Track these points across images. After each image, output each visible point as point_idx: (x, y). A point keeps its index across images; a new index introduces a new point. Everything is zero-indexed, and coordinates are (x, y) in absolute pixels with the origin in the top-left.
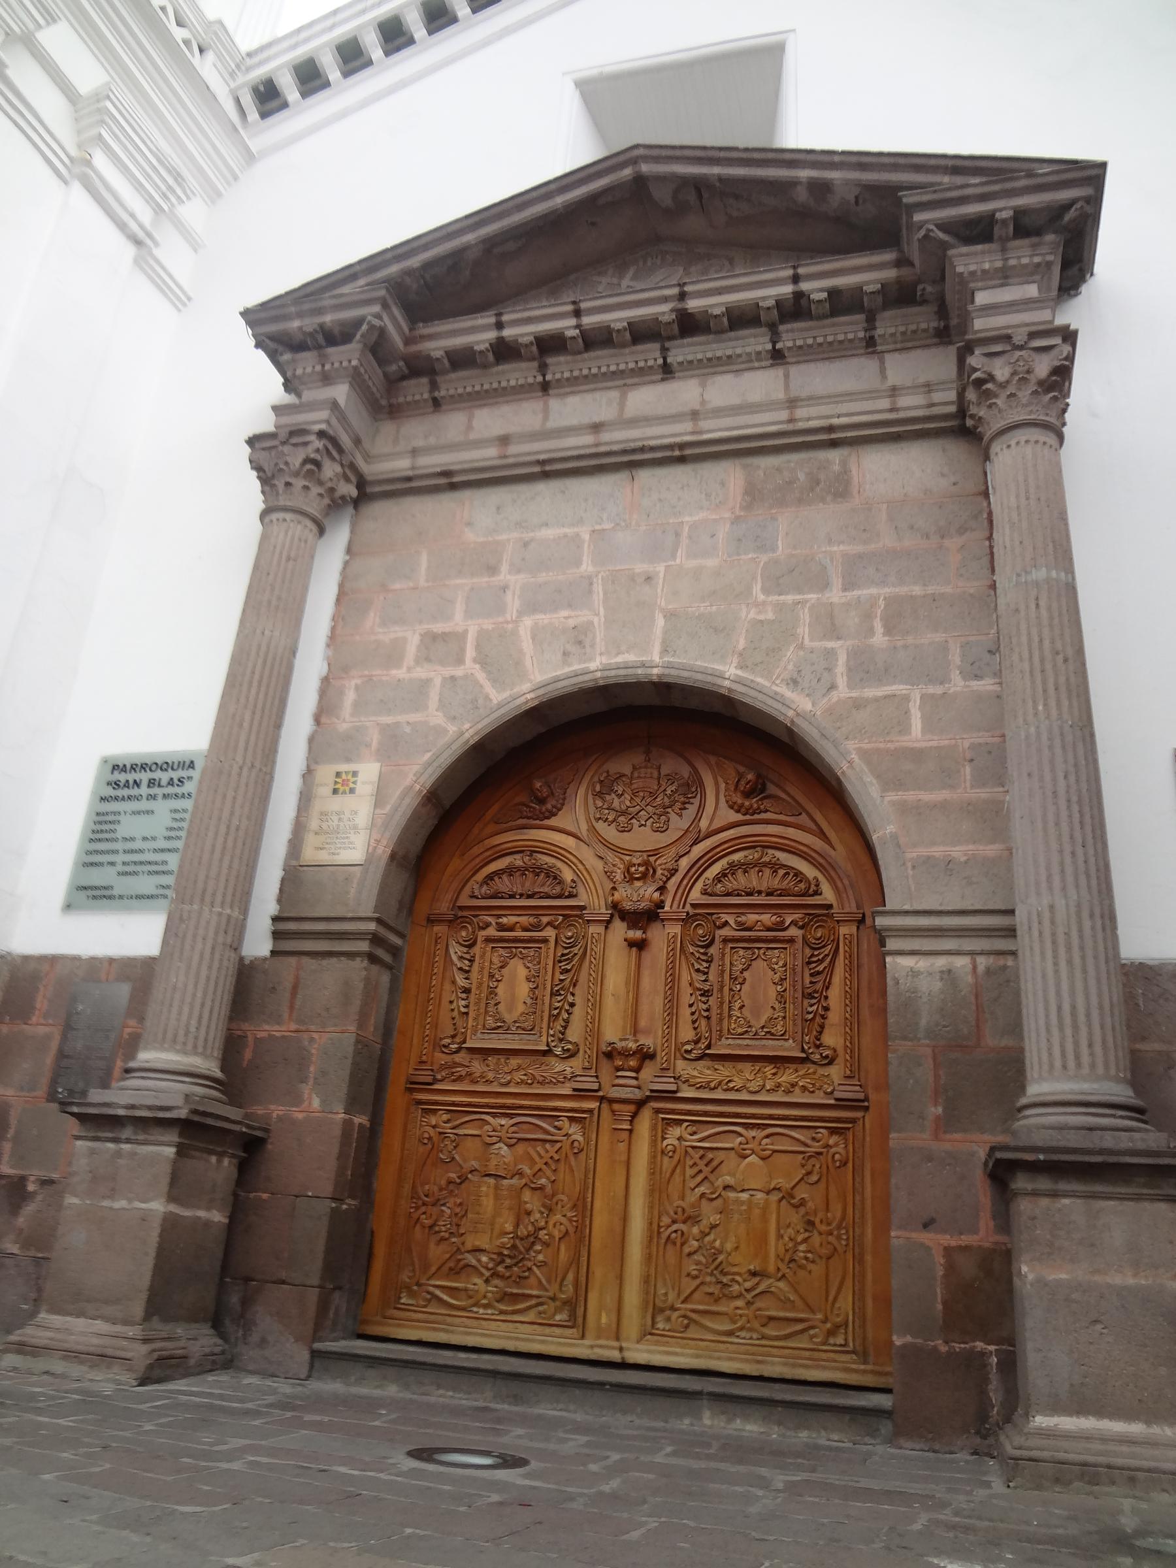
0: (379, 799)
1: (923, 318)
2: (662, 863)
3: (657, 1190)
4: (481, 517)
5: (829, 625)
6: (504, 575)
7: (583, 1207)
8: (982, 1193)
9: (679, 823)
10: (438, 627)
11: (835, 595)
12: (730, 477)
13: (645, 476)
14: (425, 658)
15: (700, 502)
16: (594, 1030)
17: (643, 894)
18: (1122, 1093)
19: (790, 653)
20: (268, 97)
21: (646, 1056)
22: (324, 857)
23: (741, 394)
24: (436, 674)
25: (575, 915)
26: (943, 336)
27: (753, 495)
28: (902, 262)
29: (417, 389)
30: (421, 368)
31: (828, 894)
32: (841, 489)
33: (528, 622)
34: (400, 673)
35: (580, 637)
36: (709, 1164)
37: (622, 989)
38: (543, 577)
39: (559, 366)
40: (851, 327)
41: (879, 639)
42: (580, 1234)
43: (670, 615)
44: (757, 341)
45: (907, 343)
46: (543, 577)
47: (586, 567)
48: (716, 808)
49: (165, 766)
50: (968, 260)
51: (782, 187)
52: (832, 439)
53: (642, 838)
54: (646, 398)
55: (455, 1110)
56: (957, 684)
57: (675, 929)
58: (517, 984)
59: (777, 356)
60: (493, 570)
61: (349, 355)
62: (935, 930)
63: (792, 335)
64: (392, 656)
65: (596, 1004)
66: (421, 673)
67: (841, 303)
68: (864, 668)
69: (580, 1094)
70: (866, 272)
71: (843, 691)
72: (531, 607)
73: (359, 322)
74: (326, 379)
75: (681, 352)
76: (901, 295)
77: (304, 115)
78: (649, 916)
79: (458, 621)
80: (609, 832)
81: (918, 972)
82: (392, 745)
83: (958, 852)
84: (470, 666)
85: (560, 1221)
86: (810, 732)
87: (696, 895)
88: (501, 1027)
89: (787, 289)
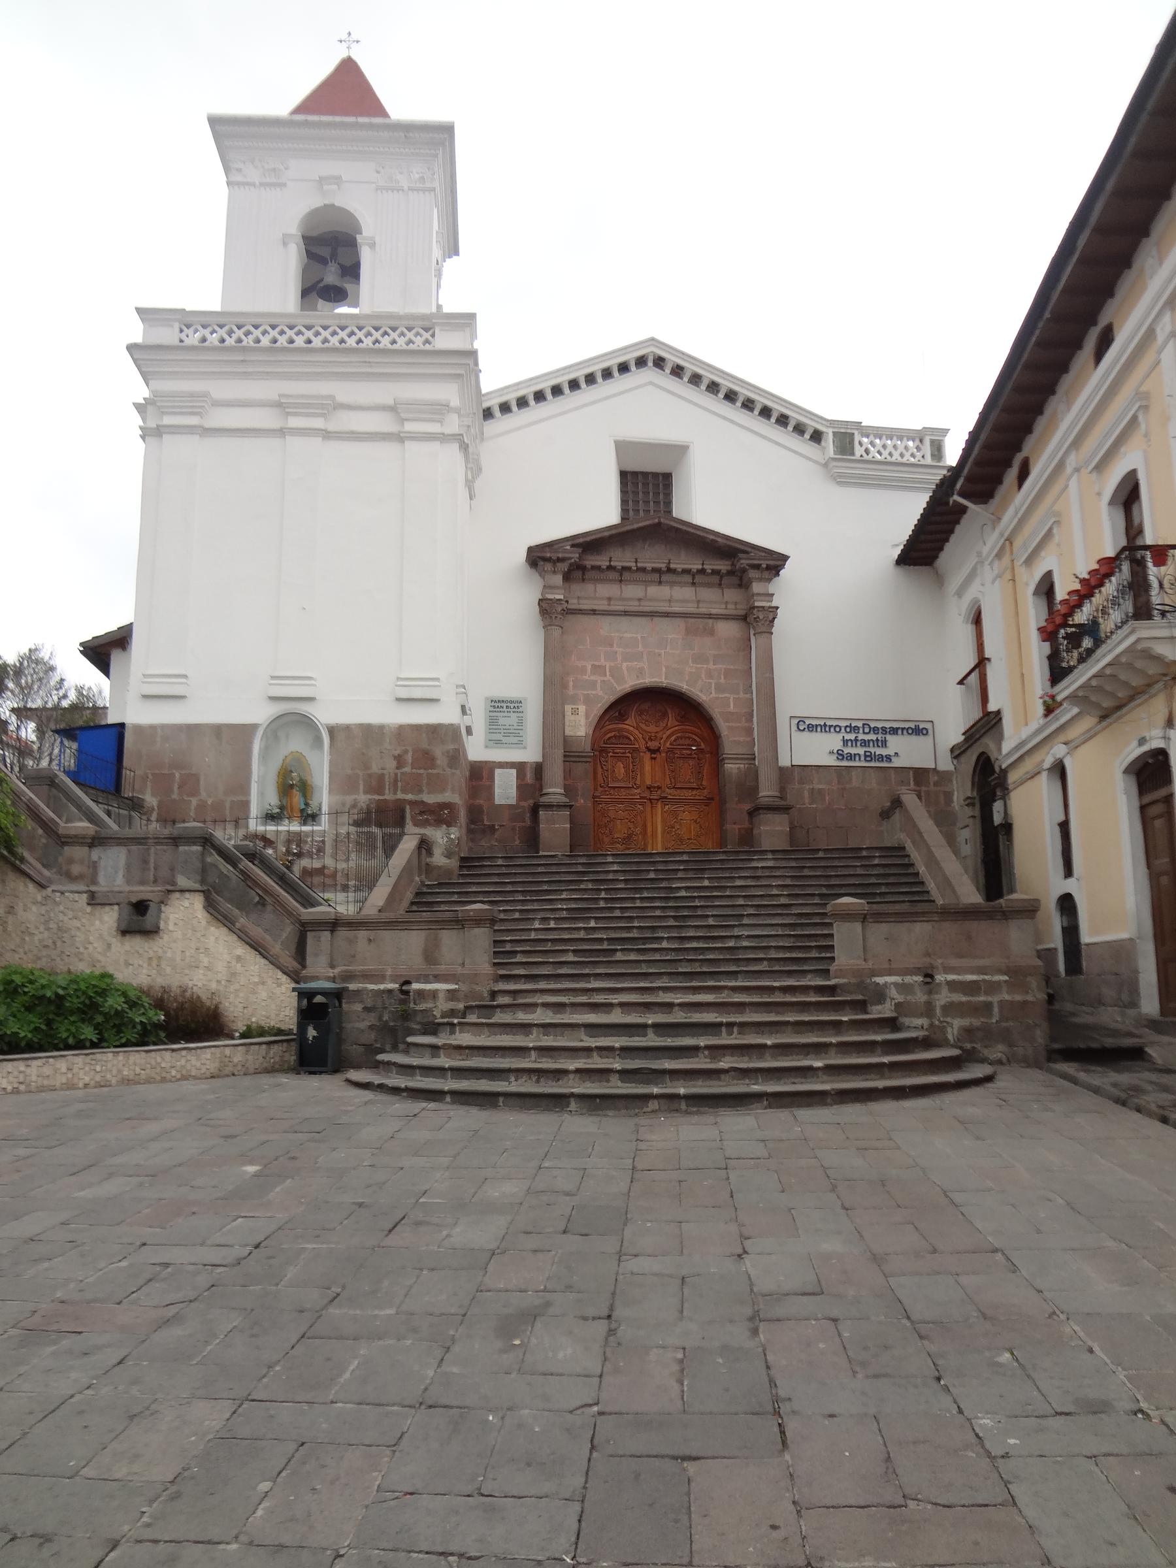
0: (587, 716)
1: (735, 580)
2: (659, 735)
3: (664, 821)
4: (605, 626)
5: (709, 674)
6: (615, 648)
7: (645, 826)
8: (746, 817)
9: (662, 724)
10: (597, 663)
11: (711, 666)
12: (680, 623)
13: (655, 619)
14: (593, 673)
15: (672, 631)
16: (643, 780)
17: (653, 745)
18: (778, 794)
19: (700, 682)
20: (488, 414)
21: (659, 788)
22: (571, 734)
23: (681, 596)
24: (599, 679)
25: (636, 750)
26: (740, 586)
27: (688, 631)
28: (733, 565)
29: (579, 574)
30: (583, 568)
31: (703, 746)
32: (712, 632)
33: (625, 664)
34: (586, 677)
35: (641, 672)
36: (675, 814)
37: (649, 771)
38: (628, 650)
39: (626, 575)
40: (716, 579)
41: (722, 680)
42: (644, 832)
43: (667, 667)
44: (689, 578)
45: (730, 586)
46: (628, 650)
47: (640, 649)
48: (671, 720)
49: (512, 702)
50: (752, 574)
51: (704, 538)
52: (710, 616)
53: (652, 728)
54: (653, 590)
55: (606, 803)
56: (741, 695)
57: (664, 754)
58: (620, 769)
59: (693, 584)
60: (611, 645)
61: (564, 567)
62: (736, 758)
63: (698, 579)
64: (583, 671)
65: (642, 774)
66: (593, 678)
67: (715, 572)
68: (719, 688)
69: (642, 798)
70: (723, 566)
71: (714, 695)
72: (625, 660)
73: (570, 558)
74: (554, 572)
75: (664, 578)
76: (731, 573)
77: (502, 423)
78: (658, 750)
79: (602, 662)
80: (643, 726)
81: (732, 768)
82: (588, 701)
83: (742, 739)
84: (608, 677)
85: (638, 830)
86: (706, 706)
87: (668, 745)
88: (619, 781)
89: (700, 567)
